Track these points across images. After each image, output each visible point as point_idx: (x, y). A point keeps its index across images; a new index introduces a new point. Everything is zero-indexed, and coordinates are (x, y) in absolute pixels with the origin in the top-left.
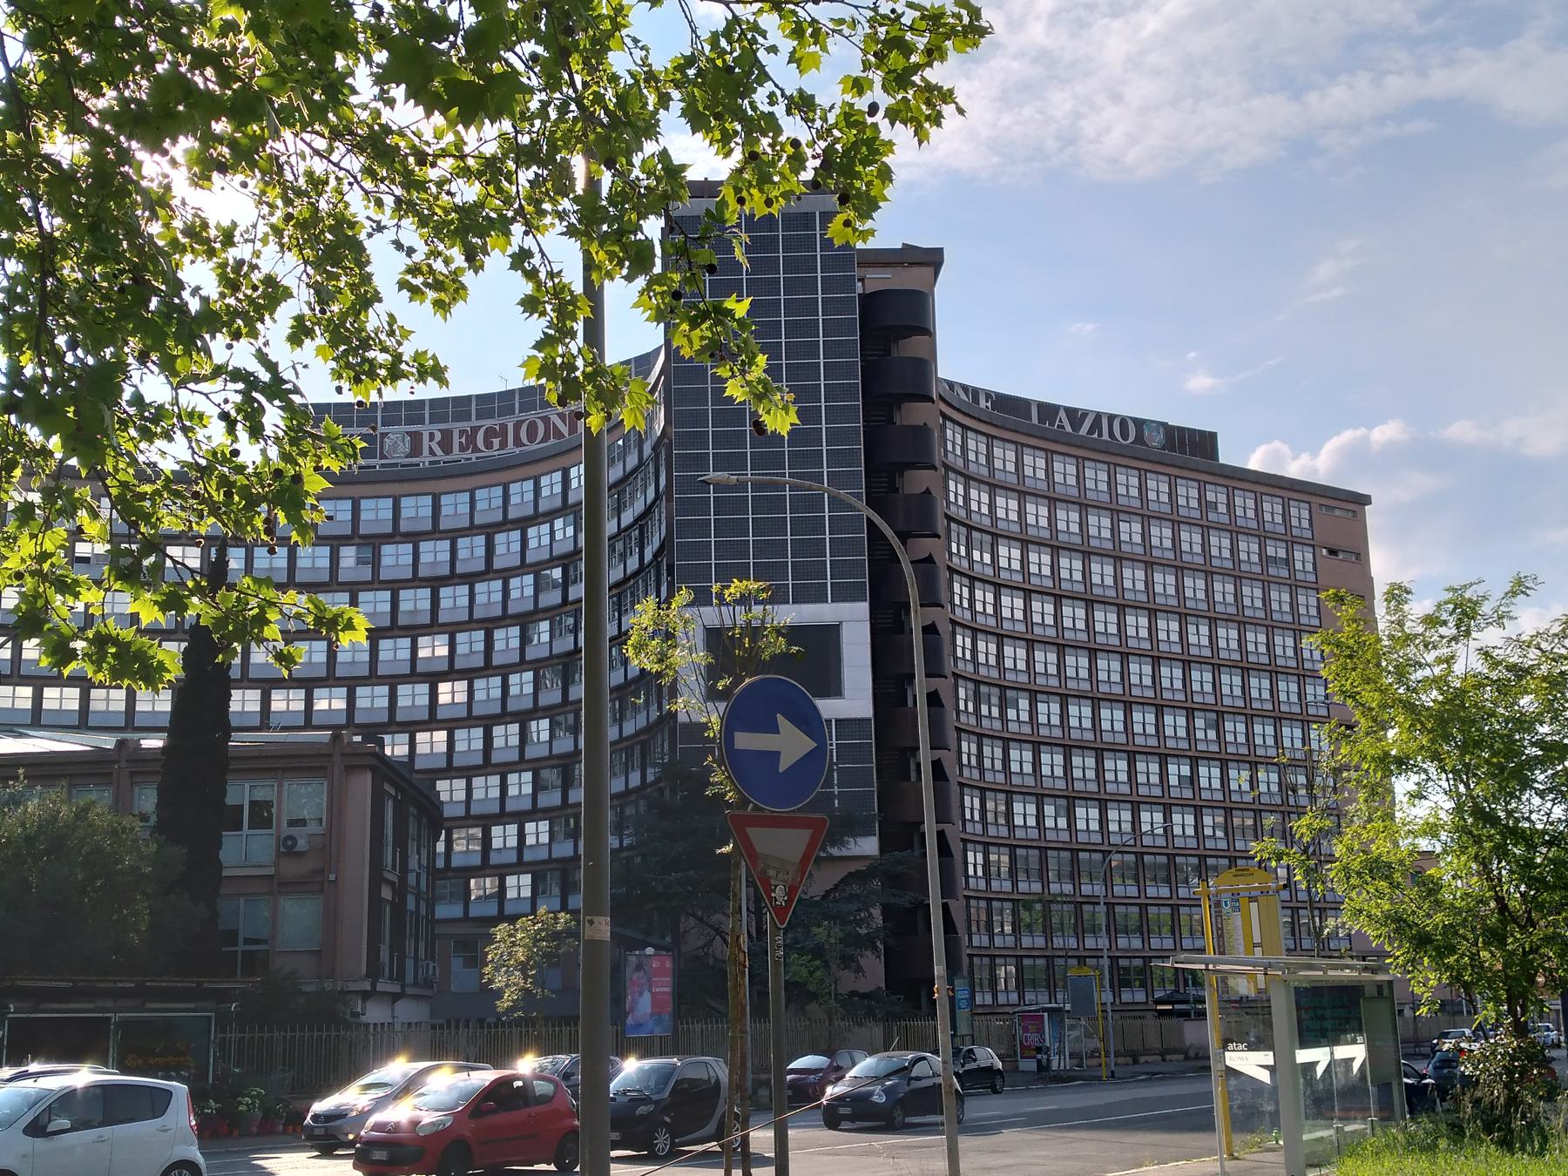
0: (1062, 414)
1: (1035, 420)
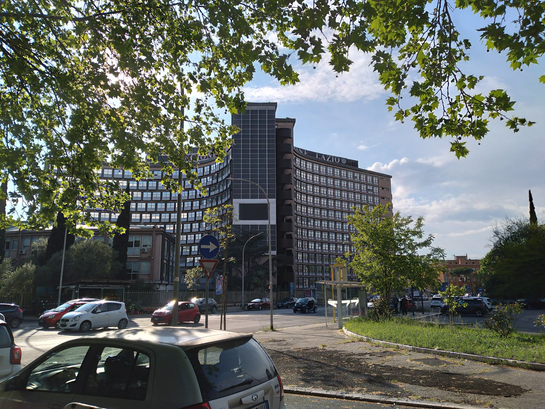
1: (317, 157)
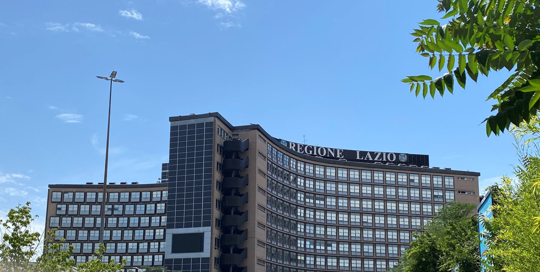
0: (368, 154)
1: (358, 158)
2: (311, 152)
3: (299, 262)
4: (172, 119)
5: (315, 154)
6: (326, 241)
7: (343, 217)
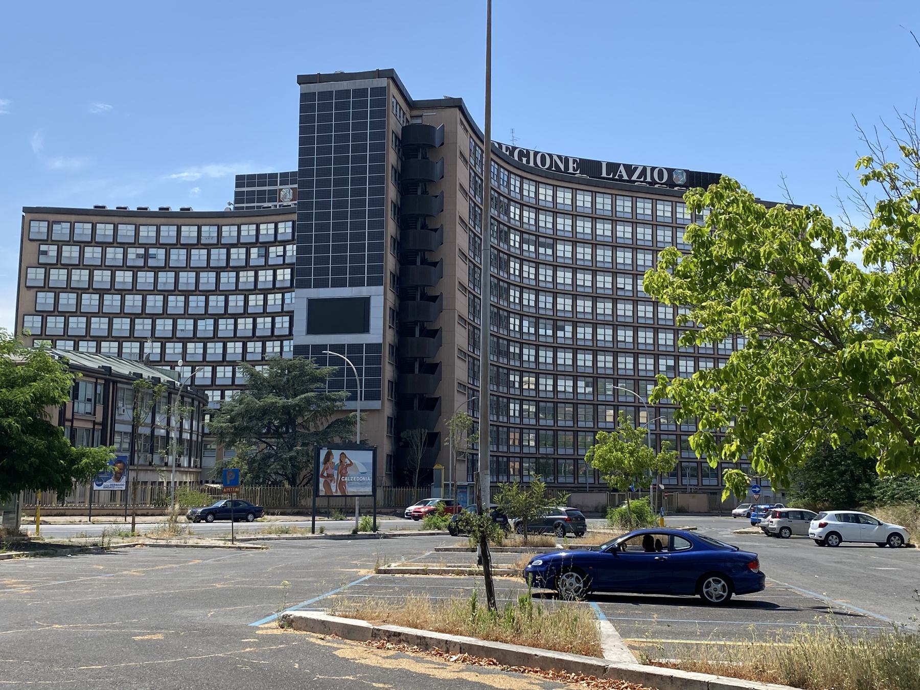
0: (622, 168)
2: (524, 160)
3: (511, 356)
4: (303, 80)
5: (532, 164)
6: (555, 321)
7: (584, 279)
